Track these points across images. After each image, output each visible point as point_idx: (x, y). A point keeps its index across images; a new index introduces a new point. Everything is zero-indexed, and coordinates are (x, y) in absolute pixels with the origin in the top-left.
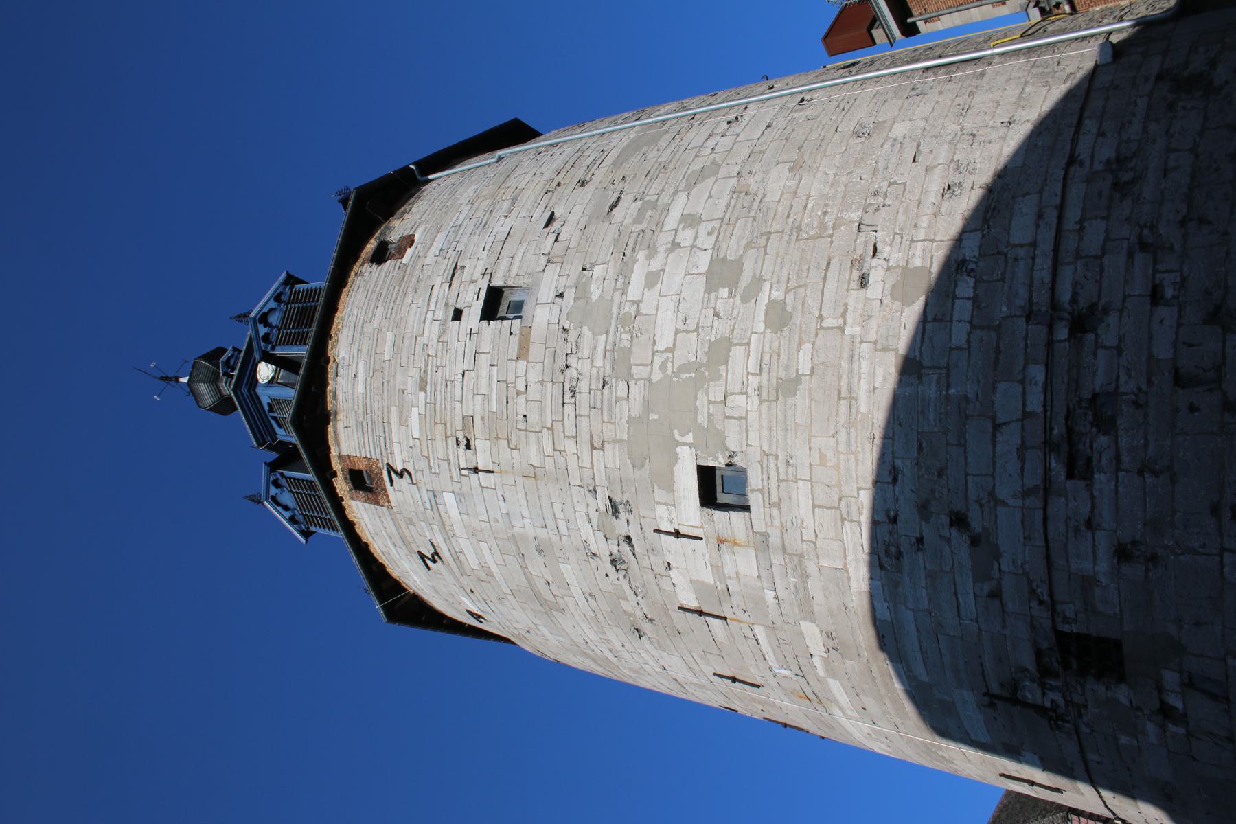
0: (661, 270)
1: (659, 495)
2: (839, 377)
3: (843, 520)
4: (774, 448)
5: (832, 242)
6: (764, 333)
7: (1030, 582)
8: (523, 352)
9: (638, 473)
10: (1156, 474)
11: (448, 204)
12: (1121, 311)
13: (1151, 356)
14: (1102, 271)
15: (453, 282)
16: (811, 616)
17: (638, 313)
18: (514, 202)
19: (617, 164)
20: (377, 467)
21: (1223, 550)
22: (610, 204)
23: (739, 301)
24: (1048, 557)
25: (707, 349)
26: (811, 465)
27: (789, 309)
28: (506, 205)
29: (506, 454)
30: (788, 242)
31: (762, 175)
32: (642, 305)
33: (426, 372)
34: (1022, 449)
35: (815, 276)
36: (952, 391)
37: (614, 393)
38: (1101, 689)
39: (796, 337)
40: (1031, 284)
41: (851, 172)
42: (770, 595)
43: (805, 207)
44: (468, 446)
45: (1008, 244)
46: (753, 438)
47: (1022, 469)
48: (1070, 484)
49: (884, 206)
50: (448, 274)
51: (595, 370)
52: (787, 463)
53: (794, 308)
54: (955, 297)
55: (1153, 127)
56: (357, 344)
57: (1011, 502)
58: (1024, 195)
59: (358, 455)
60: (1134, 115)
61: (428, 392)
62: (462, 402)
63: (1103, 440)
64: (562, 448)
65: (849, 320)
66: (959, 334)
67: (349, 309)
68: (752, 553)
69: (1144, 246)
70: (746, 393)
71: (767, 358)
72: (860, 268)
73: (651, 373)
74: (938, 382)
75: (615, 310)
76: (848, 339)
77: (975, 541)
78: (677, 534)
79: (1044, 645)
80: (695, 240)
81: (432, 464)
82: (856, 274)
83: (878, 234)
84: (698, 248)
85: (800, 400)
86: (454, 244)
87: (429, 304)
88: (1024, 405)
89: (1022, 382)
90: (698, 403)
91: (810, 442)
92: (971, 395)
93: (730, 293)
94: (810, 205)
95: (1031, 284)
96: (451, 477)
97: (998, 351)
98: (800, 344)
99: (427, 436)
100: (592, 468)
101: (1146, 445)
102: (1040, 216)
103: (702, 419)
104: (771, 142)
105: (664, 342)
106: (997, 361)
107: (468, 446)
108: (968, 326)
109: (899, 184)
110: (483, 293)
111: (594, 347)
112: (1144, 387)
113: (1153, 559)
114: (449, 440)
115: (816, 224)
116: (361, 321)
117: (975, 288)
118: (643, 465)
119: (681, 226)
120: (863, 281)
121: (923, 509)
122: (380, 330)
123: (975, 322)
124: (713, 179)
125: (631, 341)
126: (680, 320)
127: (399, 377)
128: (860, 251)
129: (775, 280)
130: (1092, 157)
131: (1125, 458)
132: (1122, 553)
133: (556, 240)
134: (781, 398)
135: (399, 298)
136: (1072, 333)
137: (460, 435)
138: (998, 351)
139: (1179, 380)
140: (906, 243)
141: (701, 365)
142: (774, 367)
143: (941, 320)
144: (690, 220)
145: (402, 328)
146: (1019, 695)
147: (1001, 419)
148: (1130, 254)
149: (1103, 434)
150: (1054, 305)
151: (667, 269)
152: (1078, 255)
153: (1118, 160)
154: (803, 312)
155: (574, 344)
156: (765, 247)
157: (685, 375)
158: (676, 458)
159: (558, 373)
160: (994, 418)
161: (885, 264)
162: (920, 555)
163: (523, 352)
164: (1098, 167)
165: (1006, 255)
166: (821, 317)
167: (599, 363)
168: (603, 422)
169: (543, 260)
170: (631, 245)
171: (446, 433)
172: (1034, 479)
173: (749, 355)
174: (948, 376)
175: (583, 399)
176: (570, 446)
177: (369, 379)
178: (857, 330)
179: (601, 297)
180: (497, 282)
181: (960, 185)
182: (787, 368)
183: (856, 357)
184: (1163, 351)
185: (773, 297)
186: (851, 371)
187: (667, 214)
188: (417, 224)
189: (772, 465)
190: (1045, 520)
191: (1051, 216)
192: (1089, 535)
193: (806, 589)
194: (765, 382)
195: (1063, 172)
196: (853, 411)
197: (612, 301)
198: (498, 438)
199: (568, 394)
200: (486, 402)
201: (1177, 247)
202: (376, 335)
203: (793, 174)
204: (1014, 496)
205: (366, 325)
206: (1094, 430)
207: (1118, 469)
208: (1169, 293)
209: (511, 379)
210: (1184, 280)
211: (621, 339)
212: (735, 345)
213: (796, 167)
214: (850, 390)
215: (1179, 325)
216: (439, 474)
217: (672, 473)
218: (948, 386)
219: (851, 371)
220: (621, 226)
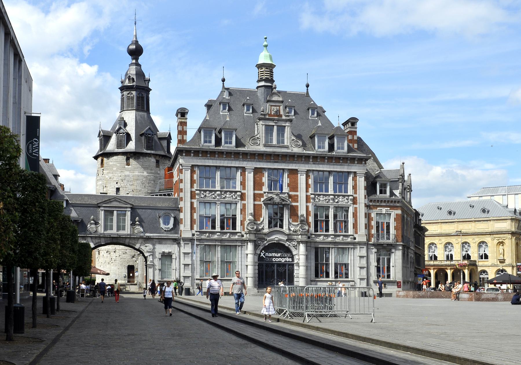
28: (131, 184)
110: (119, 187)
127: (111, 172)
180: (120, 189)
184: (113, 257)
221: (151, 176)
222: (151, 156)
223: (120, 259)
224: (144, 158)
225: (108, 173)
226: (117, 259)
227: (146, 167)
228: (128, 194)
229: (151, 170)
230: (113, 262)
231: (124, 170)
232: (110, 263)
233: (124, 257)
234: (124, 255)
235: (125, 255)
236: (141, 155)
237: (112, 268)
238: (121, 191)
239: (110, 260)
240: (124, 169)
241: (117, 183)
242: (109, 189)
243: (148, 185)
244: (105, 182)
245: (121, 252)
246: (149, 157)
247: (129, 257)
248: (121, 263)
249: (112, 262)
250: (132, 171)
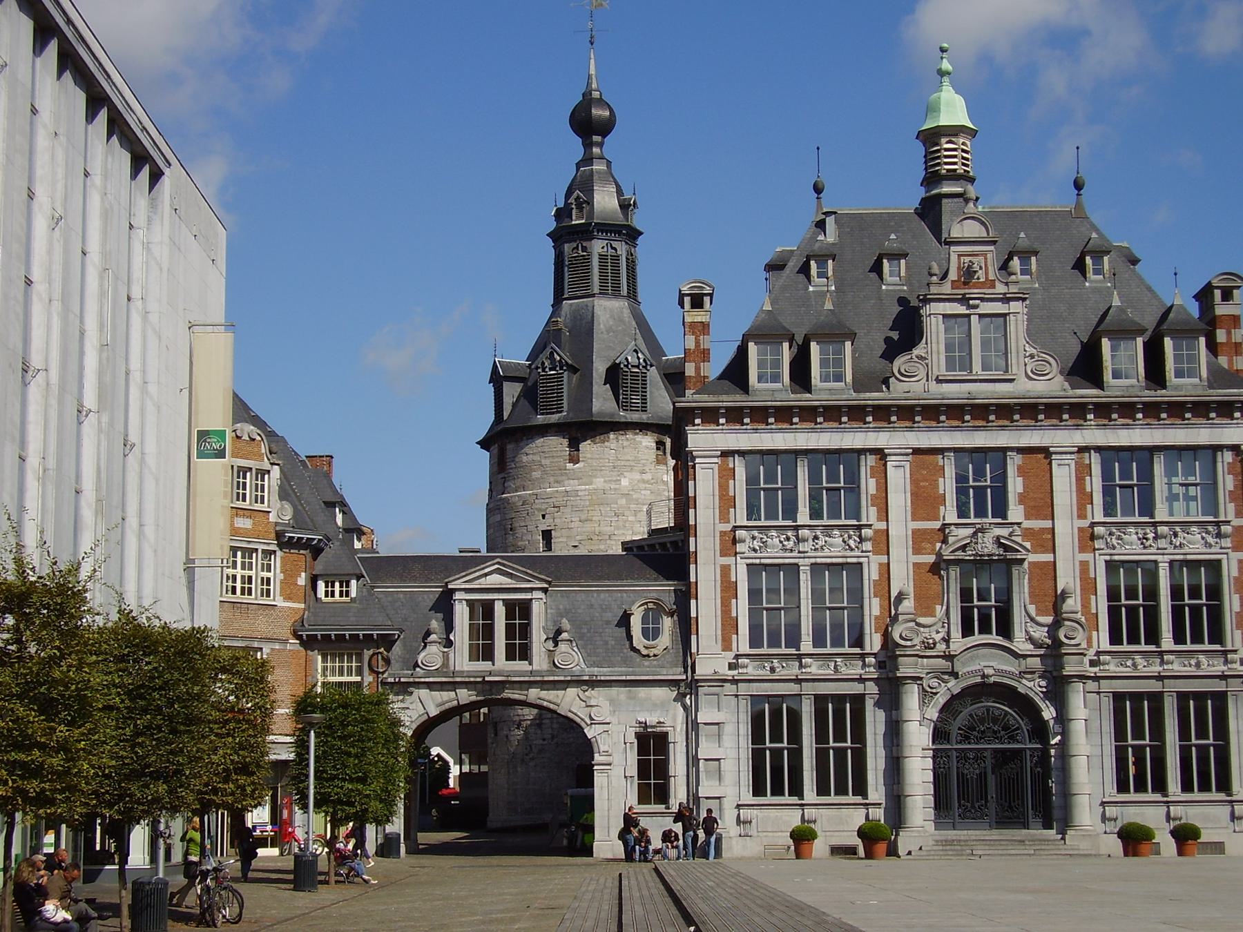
110: (549, 528)
224: (620, 437)
227: (627, 463)
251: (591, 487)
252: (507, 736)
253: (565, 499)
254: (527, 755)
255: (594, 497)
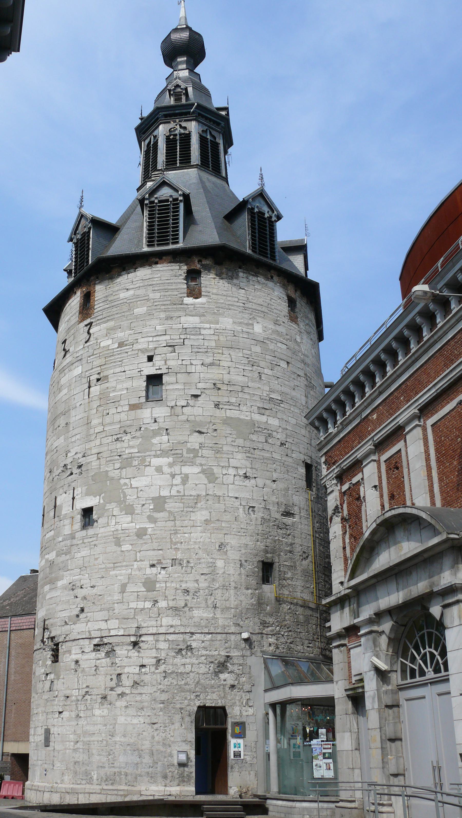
0: (163, 473)
1: (84, 488)
2: (120, 562)
3: (80, 568)
4: (99, 539)
5: (168, 549)
6: (136, 528)
7: (69, 634)
8: (133, 407)
9: (90, 478)
10: (96, 670)
11: (221, 309)
12: (138, 656)
13: (125, 666)
14: (151, 649)
15: (167, 347)
16: (57, 556)
17: (146, 466)
18: (212, 364)
19: (227, 421)
20: (91, 314)
21: (79, 689)
22: (200, 430)
23: (148, 514)
24: (75, 640)
25: (131, 504)
26: (94, 555)
27: (144, 537)
28: (209, 360)
29: (95, 404)
30: (171, 530)
31: (205, 507)
32: (148, 467)
33: (126, 345)
34: (100, 630)
35: (155, 545)
36: (116, 605)
37: (116, 462)
38: (49, 656)
39: (134, 543)
40: (148, 627)
41: (200, 548)
42: (60, 539)
43: (185, 533)
44: (98, 380)
45: (162, 617)
46: (102, 530)
47: (95, 630)
48: (92, 646)
49: (182, 567)
50: (171, 343)
51: (124, 449)
52: (95, 545)
53: (144, 540)
54: (145, 601)
55: (203, 658)
56: (141, 285)
57: (87, 627)
58: (180, 619)
59: (96, 299)
60: (210, 651)
61: (117, 350)
62: (113, 374)
63: (103, 654)
64: (97, 437)
65: (139, 563)
66: (133, 605)
67: (161, 269)
68: (70, 532)
69: (159, 661)
70: (116, 525)
71: (127, 531)
72: (158, 563)
73: (123, 478)
74: (119, 599)
75: (148, 453)
76: (132, 563)
77: (78, 616)
78: (73, 498)
79: (56, 639)
80: (175, 485)
81: (91, 357)
82: (155, 562)
83: (170, 568)
84: (171, 489)
85: (115, 548)
86: (188, 336)
87: (156, 336)
88: (112, 629)
89: (119, 628)
90: (113, 503)
91: (101, 553)
92: (114, 612)
93: (152, 509)
94: (186, 535)
95: (148, 627)
96: (86, 371)
97: (128, 619)
98: (131, 545)
99: (101, 353)
100: (91, 455)
101: (102, 667)
102: (172, 626)
103: (108, 506)
104: (225, 504)
105: (135, 483)
106: (125, 619)
107: (98, 380)
108: (135, 607)
109: (191, 571)
110: (159, 372)
111: (133, 447)
112: (117, 665)
113: (76, 671)
114: (99, 368)
115: (177, 540)
116: (154, 283)
117: (148, 608)
118: (93, 480)
119: (183, 476)
120: (153, 566)
121: (85, 598)
122: (148, 300)
123: (137, 610)
124: (206, 482)
125: (135, 466)
126: (142, 488)
127: (125, 324)
128: (164, 562)
129: (155, 528)
130: (194, 640)
131: (99, 661)
132: (77, 662)
133: (183, 407)
134: (114, 540)
135: (163, 307)
136: (132, 642)
137: (102, 375)
138: (128, 619)
139: (119, 674)
140: (165, 579)
141: (125, 502)
142: (124, 535)
143: (138, 597)
144: (185, 479)
145: (148, 317)
146: (46, 630)
147: (109, 622)
148: (155, 657)
149: (105, 655)
150: (140, 636)
151: (163, 475)
152: (157, 641)
153: (192, 649)
154: (142, 544)
155: (134, 436)
156: (169, 520)
157: (122, 495)
158: (95, 497)
159: (123, 429)
160: (108, 620)
161: (158, 573)
162: (73, 597)
163: (133, 407)
164: (189, 644)
165: (158, 617)
166: (140, 551)
167: (127, 452)
168: (106, 458)
169: (173, 404)
170: (176, 452)
171: (102, 365)
172: (94, 634)
173: (128, 523)
174: (120, 603)
175: (113, 447)
176: (98, 442)
177: (125, 301)
178: (135, 567)
179: (153, 444)
180: (165, 379)
181: (188, 595)
182: (124, 540)
183: (127, 568)
184: (126, 670)
185: (148, 529)
186: (122, 566)
187: (189, 466)
188: (208, 294)
189: (95, 539)
190: (83, 639)
191: (172, 630)
192: (80, 652)
193: (63, 554)
194: (119, 532)
195: (188, 631)
196: (110, 569)
197: (151, 451)
198: (100, 399)
199: (115, 437)
200: (114, 389)
201: (157, 671)
202: (146, 298)
203: (203, 522)
204: (89, 628)
205: (151, 288)
206: (106, 652)
207: (96, 659)
208: (143, 670)
209: (122, 403)
210: (147, 674)
211: (136, 460)
212: (132, 517)
213: (207, 522)
214: (117, 567)
215: (134, 674)
216: (87, 363)
217: (90, 495)
218: (117, 603)
219: (122, 566)
220: (187, 442)
221: (279, 345)
222: (272, 277)
223: (159, 677)
224: (251, 277)
225: (109, 331)
226: (147, 678)
228: (196, 396)
229: (276, 323)
230: (127, 691)
231: (177, 314)
232: (112, 695)
233: (181, 669)
234: (179, 660)
235: (184, 661)
236: (240, 268)
237: (121, 720)
238: (170, 387)
239: (113, 684)
240: (178, 310)
241: (150, 359)
242: (114, 384)
243: (270, 372)
244: (97, 362)
245: (163, 645)
246: (267, 279)
247: (203, 669)
248: (164, 697)
249: (119, 690)
250: (209, 317)
251: (218, 327)
252: (77, 662)
253: (182, 337)
254: (112, 689)
255: (221, 338)
